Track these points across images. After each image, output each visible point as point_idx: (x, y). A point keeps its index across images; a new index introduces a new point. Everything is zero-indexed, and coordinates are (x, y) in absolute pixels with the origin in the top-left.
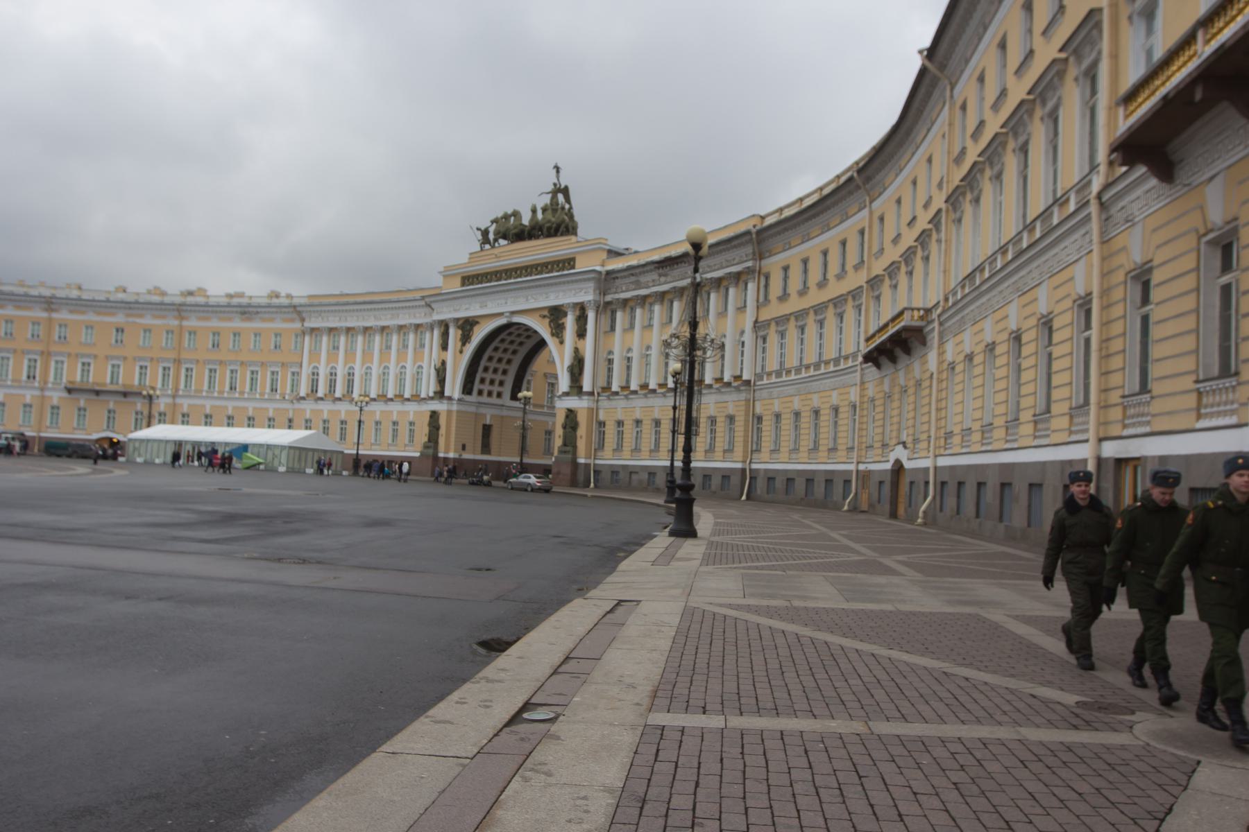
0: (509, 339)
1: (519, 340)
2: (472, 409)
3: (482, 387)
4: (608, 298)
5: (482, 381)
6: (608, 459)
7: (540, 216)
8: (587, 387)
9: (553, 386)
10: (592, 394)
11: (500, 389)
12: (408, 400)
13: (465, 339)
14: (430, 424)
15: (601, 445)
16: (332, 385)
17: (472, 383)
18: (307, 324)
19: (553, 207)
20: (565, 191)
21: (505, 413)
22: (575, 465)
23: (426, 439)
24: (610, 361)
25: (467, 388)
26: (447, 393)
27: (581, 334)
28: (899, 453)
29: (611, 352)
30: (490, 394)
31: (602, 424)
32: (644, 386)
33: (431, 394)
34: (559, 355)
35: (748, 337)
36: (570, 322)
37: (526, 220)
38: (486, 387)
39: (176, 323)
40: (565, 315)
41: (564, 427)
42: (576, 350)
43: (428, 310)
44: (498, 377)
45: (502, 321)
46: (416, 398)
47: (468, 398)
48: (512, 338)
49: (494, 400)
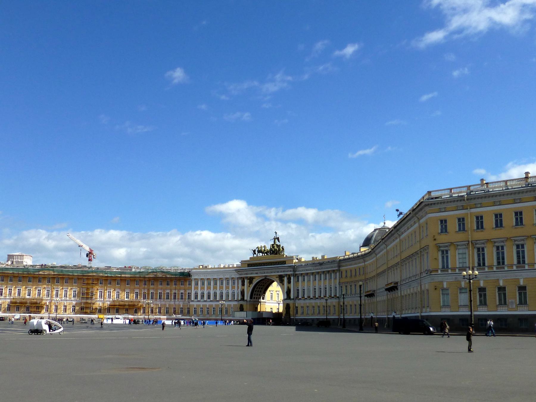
4: (297, 273)
6: (299, 317)
8: (292, 297)
10: (293, 299)
13: (251, 283)
15: (297, 313)
20: (278, 239)
22: (291, 319)
26: (245, 299)
28: (372, 315)
31: (297, 307)
32: (309, 297)
33: (240, 299)
35: (338, 286)
36: (285, 279)
42: (288, 287)
45: (264, 278)
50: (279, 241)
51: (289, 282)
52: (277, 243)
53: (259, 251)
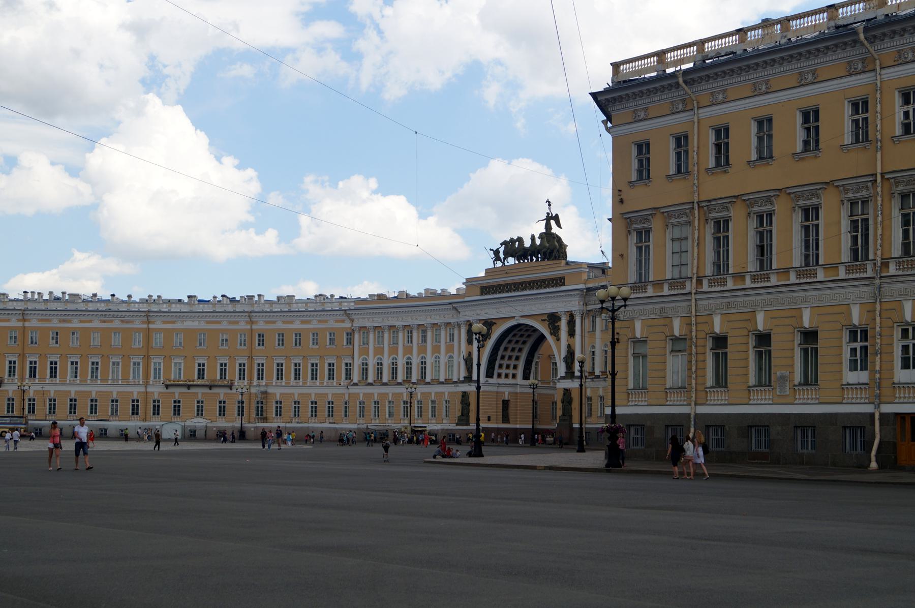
0: (520, 333)
1: (527, 334)
2: (494, 389)
3: (500, 371)
4: (589, 308)
5: (501, 366)
7: (538, 242)
8: (577, 374)
9: (555, 370)
11: (514, 372)
12: (442, 383)
14: (462, 402)
16: (379, 372)
17: (493, 368)
18: (355, 325)
19: (548, 235)
20: (556, 218)
21: (519, 390)
22: (572, 429)
23: (460, 414)
24: (593, 353)
25: (489, 374)
27: (572, 333)
29: (593, 347)
30: (507, 376)
33: (462, 379)
34: (557, 348)
36: (563, 325)
37: (527, 244)
38: (504, 371)
39: (248, 327)
40: (559, 319)
41: (563, 402)
42: (569, 346)
43: (454, 312)
44: (512, 362)
46: (448, 382)
47: (489, 379)
48: (522, 332)
49: (510, 381)
50: (559, 225)
51: (572, 333)
52: (555, 229)
53: (507, 254)
